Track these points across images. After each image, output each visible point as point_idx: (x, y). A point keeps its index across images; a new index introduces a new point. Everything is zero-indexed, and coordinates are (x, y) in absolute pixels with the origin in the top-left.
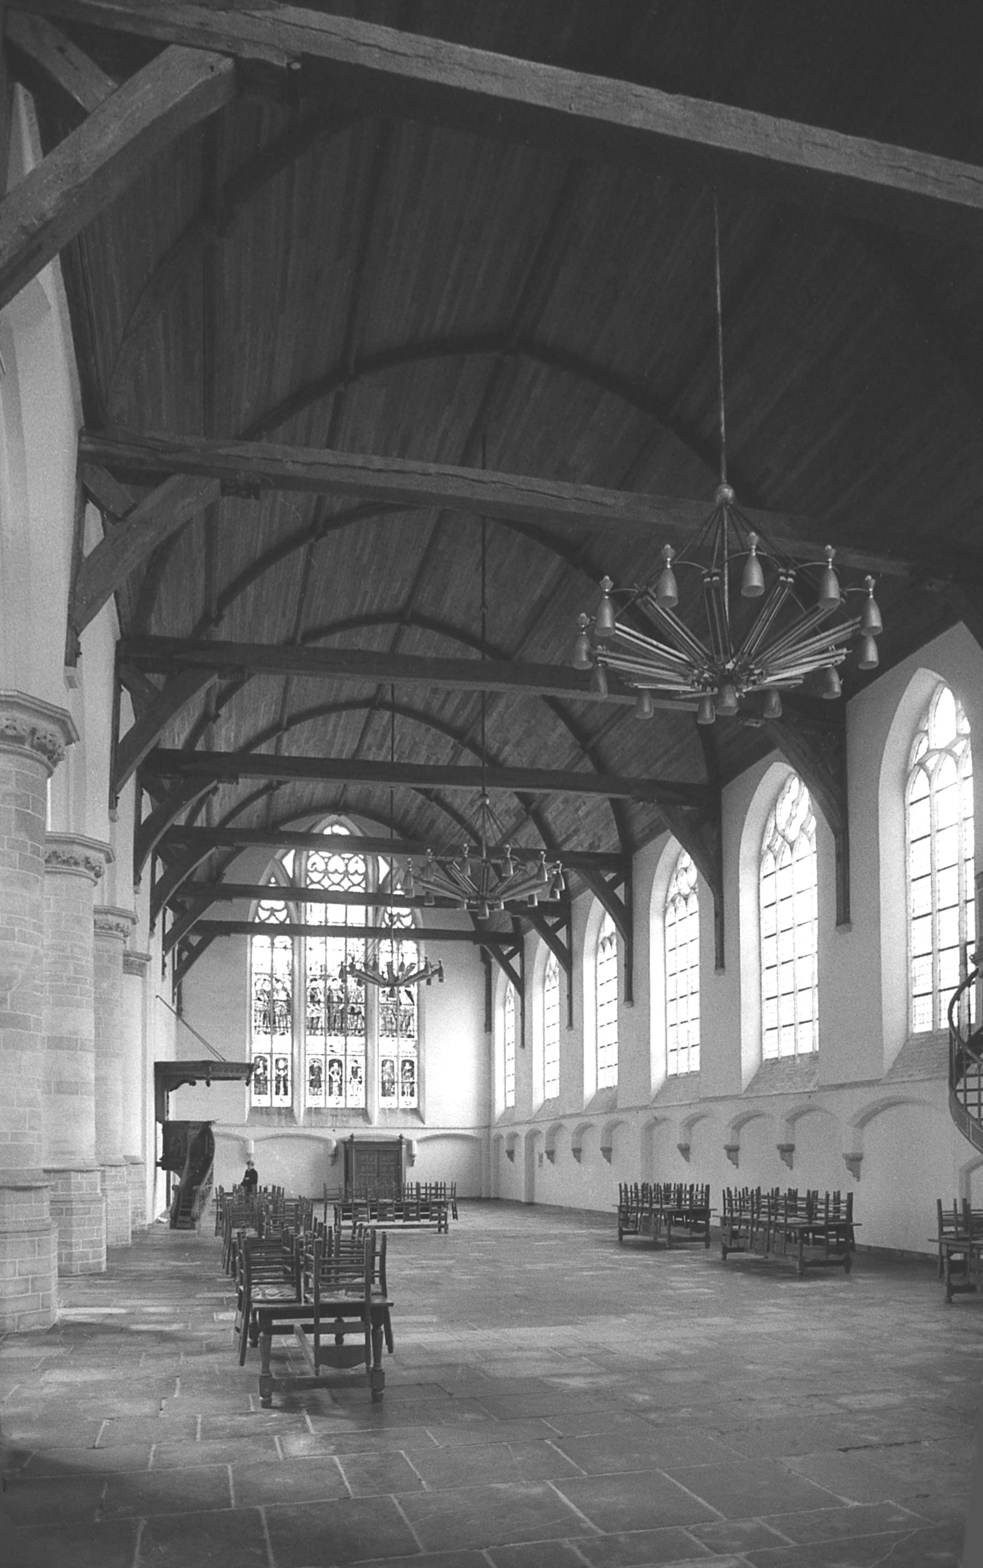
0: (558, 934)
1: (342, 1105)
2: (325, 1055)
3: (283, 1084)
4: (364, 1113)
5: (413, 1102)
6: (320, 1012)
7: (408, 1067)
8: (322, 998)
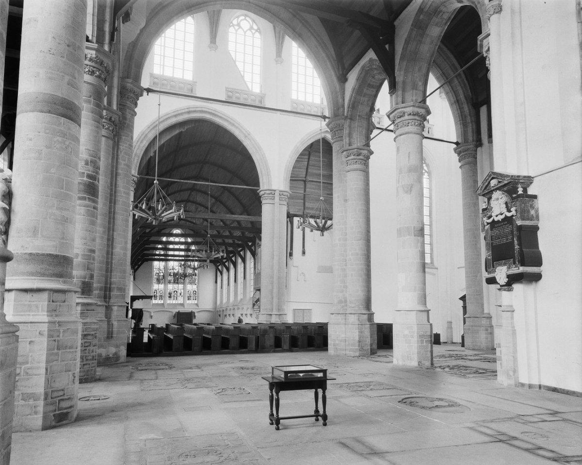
0: (226, 264)
1: (177, 303)
2: (173, 289)
3: (161, 297)
4: (182, 305)
5: (196, 302)
6: (171, 278)
7: (195, 292)
8: (172, 274)
